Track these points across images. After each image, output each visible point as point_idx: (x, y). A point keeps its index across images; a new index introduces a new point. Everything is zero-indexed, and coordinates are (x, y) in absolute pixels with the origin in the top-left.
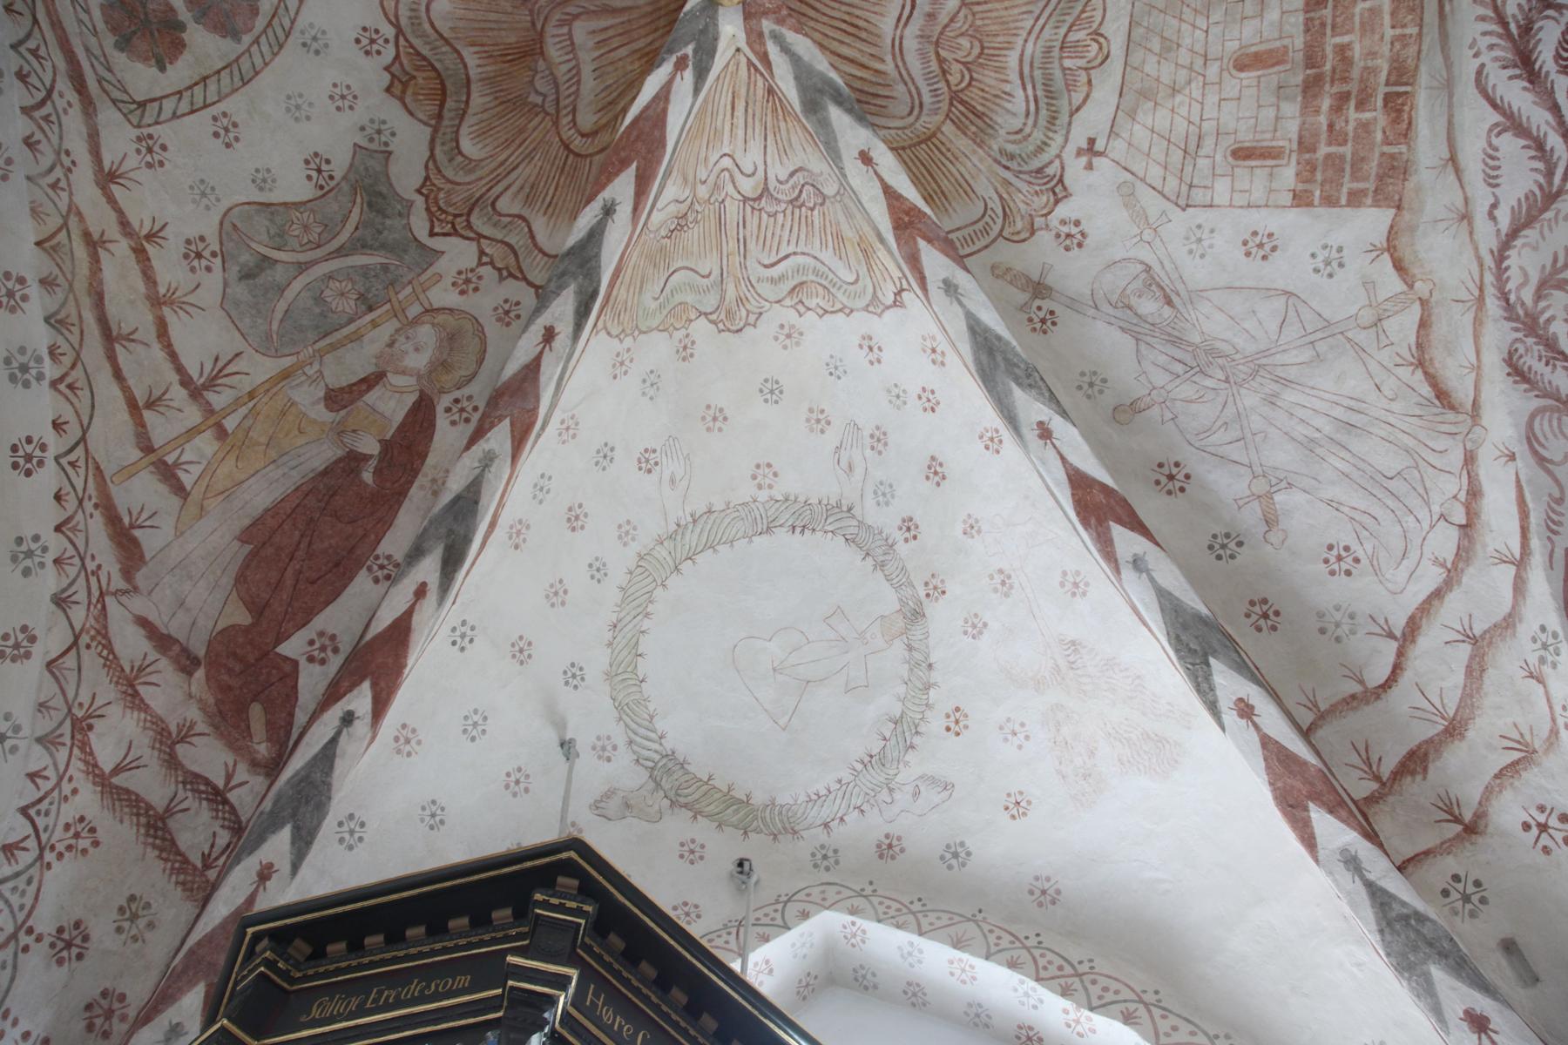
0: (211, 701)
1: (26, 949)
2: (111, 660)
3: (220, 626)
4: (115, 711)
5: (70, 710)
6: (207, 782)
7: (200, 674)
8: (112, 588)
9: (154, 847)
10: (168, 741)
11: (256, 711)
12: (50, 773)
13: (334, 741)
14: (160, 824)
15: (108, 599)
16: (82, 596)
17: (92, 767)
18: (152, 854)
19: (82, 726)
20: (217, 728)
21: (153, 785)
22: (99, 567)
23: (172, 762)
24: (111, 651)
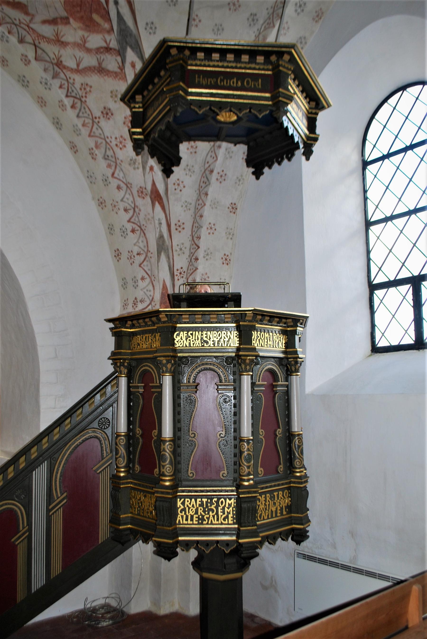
0: (81, 25)
1: (98, 122)
2: (48, 40)
3: (63, 3)
4: (62, 52)
5: (52, 63)
6: (102, 48)
7: (71, 20)
8: (28, 21)
9: (105, 75)
10: (82, 45)
11: (95, 17)
12: (63, 82)
13: (118, 13)
14: (101, 69)
15: (32, 25)
16: (24, 33)
17: (72, 70)
18: (106, 78)
19: (59, 64)
20: (90, 31)
21: (89, 61)
22: (19, 20)
23: (89, 51)
24: (45, 38)
